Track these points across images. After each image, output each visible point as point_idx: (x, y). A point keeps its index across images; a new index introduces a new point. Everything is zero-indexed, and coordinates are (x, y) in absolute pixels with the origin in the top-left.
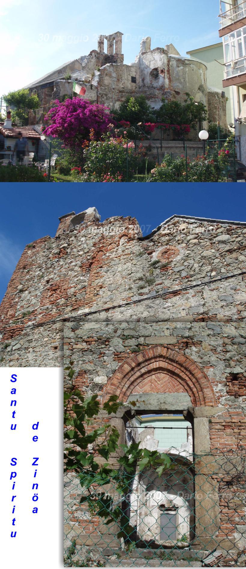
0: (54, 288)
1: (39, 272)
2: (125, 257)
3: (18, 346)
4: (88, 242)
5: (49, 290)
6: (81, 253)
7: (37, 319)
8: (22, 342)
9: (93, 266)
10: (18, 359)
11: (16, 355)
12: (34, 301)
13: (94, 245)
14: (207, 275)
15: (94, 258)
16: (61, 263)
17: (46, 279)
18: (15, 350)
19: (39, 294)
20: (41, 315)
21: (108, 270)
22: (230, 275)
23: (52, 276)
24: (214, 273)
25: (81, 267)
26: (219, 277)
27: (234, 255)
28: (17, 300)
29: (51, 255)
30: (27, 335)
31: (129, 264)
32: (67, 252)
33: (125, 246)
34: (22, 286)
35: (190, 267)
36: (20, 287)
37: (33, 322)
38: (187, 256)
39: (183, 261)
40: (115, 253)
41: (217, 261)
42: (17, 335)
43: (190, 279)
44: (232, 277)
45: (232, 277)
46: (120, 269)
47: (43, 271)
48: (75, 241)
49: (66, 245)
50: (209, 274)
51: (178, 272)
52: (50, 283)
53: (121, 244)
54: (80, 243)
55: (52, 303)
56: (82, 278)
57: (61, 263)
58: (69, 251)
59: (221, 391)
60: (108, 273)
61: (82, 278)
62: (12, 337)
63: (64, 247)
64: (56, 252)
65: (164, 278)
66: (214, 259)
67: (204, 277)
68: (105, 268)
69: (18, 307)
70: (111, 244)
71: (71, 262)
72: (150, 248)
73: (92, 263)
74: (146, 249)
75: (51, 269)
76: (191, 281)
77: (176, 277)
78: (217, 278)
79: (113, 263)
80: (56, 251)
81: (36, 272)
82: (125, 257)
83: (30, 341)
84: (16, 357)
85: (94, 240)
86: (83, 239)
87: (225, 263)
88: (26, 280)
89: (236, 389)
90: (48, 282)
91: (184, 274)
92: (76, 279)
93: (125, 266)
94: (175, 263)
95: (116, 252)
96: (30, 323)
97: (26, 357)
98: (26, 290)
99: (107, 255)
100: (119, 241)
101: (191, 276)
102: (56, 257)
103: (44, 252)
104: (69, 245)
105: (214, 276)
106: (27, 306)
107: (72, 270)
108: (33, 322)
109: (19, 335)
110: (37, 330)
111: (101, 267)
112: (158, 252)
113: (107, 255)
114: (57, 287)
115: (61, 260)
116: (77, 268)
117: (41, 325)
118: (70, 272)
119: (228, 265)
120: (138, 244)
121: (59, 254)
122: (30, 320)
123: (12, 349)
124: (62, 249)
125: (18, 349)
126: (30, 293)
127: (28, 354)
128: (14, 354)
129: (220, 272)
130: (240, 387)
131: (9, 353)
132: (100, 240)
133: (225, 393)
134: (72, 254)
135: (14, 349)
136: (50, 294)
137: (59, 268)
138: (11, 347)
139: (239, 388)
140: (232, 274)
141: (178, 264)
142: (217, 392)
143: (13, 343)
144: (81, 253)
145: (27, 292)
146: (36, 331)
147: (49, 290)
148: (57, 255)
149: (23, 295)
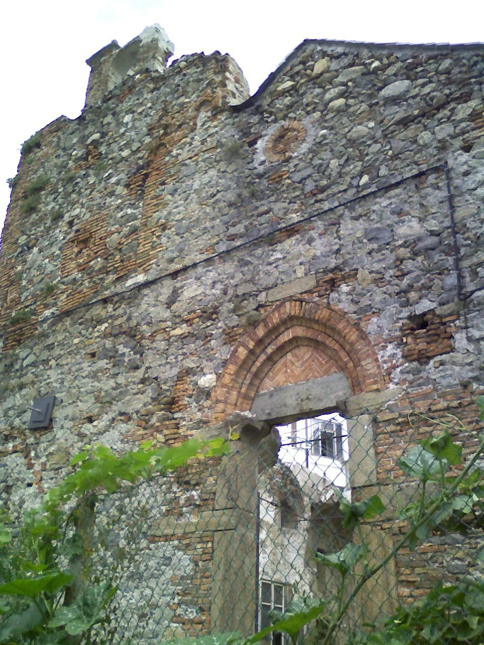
0: (81, 237)
1: (53, 204)
2: (207, 155)
3: (31, 359)
4: (137, 124)
5: (73, 242)
6: (125, 153)
7: (59, 304)
8: (36, 349)
9: (150, 182)
10: (33, 383)
11: (30, 375)
12: (50, 268)
13: (151, 129)
14: (350, 186)
15: (148, 164)
16: (91, 180)
17: (67, 217)
18: (27, 366)
19: (58, 252)
20: (65, 296)
21: (176, 190)
22: (393, 181)
23: (77, 211)
24: (365, 179)
25: (127, 186)
26: (373, 189)
27: (410, 132)
28: (19, 268)
29: (71, 163)
30: (44, 335)
31: (213, 173)
32: (100, 154)
33: (207, 129)
34: (25, 237)
35: (323, 168)
36: (23, 240)
37: (51, 311)
38: (320, 143)
39: (310, 156)
40: (187, 148)
41: (376, 147)
42: (28, 338)
43: (320, 196)
44: (397, 184)
45: (397, 184)
46: (196, 186)
47: (60, 201)
48: (113, 125)
49: (96, 136)
50: (355, 183)
51: (300, 182)
52: (75, 228)
53: (199, 124)
54: (122, 130)
55: (82, 268)
56: (129, 211)
57: (91, 180)
58: (103, 149)
59: (393, 356)
60: (176, 196)
61: (129, 211)
62: (19, 342)
63: (94, 141)
64: (80, 154)
65: (273, 199)
66: (369, 146)
67: (345, 191)
68: (170, 187)
69: (24, 283)
70: (180, 126)
71: (110, 177)
72: (252, 130)
73: (147, 176)
74: (246, 134)
75: (74, 196)
76: (321, 200)
77: (294, 195)
78: (369, 191)
79: (185, 171)
80: (78, 152)
81: (47, 205)
82: (207, 155)
83: (50, 347)
84: (31, 380)
85: (148, 119)
86: (127, 118)
87: (390, 153)
88: (32, 223)
89: (422, 346)
90: (71, 224)
91: (310, 186)
92: (120, 215)
93: (206, 178)
94: (296, 162)
95: (191, 144)
96: (47, 313)
97: (46, 377)
98: (34, 245)
99: (174, 152)
100: (195, 118)
101: (323, 190)
102: (81, 166)
103: (58, 157)
104: (103, 135)
105: (366, 186)
106: (39, 278)
107: (112, 194)
108: (51, 311)
109: (32, 336)
110: (60, 325)
111: (163, 183)
112: (266, 138)
113: (174, 152)
114: (87, 235)
115: (91, 172)
116: (120, 190)
117: (67, 313)
118: (108, 200)
119: (395, 157)
120: (230, 121)
121: (86, 159)
122: (47, 306)
123: (22, 366)
124: (91, 147)
125: (34, 364)
126: (41, 251)
127: (49, 372)
128: (26, 374)
129: (378, 176)
130: (429, 340)
131: (18, 374)
132: (160, 118)
133: (401, 360)
134: (110, 156)
135: (24, 365)
136: (76, 250)
137: (88, 192)
138: (19, 362)
139: (428, 343)
140: (399, 179)
141: (302, 165)
142: (385, 362)
143: (22, 355)
144: (125, 153)
145: (35, 250)
146: (59, 327)
147: (73, 242)
148: (82, 163)
149: (30, 257)
